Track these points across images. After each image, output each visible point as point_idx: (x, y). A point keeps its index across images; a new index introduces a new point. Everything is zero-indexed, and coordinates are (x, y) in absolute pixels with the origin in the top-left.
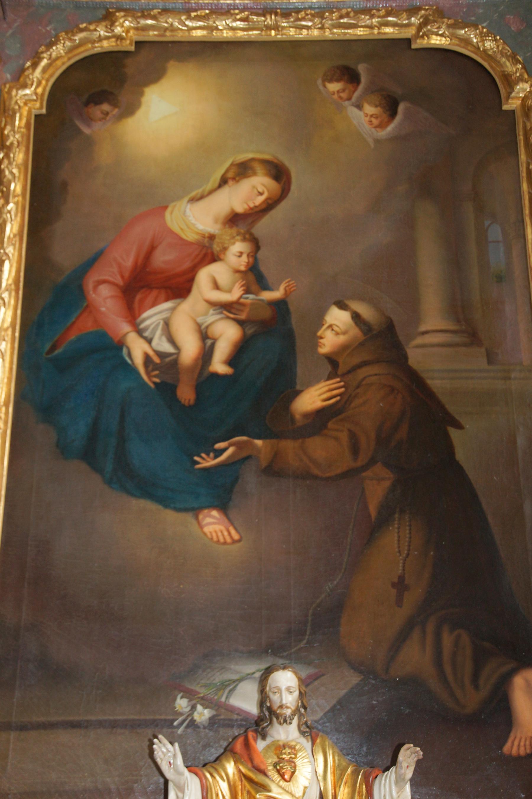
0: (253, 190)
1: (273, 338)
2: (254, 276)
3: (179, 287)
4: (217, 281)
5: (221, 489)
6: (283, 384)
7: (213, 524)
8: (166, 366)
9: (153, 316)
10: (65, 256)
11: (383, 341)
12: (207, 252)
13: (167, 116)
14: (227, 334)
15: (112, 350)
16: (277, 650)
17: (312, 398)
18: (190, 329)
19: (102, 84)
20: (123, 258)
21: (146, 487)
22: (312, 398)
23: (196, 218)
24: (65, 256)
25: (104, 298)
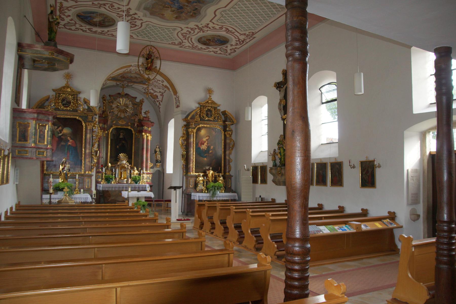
0: (207, 138)
1: (209, 147)
2: (208, 144)
3: (203, 144)
4: (206, 144)
5: (206, 157)
6: (209, 151)
7: (205, 159)
8: (203, 149)
9: (202, 146)
10: (197, 142)
11: (214, 148)
12: (205, 142)
13: (203, 132)
14: (206, 147)
15: (200, 148)
16: (208, 166)
17: (210, 152)
18: (204, 147)
19: (199, 130)
20: (200, 142)
21: (202, 157)
22: (210, 152)
23: (204, 139)
24: (197, 142)
25: (199, 144)
